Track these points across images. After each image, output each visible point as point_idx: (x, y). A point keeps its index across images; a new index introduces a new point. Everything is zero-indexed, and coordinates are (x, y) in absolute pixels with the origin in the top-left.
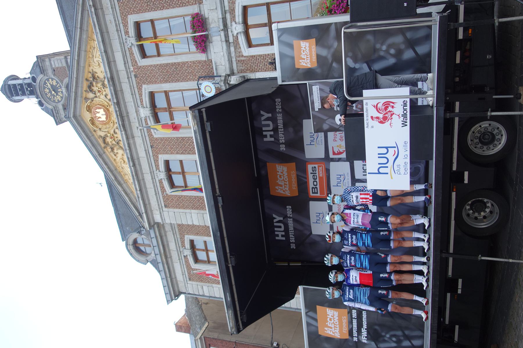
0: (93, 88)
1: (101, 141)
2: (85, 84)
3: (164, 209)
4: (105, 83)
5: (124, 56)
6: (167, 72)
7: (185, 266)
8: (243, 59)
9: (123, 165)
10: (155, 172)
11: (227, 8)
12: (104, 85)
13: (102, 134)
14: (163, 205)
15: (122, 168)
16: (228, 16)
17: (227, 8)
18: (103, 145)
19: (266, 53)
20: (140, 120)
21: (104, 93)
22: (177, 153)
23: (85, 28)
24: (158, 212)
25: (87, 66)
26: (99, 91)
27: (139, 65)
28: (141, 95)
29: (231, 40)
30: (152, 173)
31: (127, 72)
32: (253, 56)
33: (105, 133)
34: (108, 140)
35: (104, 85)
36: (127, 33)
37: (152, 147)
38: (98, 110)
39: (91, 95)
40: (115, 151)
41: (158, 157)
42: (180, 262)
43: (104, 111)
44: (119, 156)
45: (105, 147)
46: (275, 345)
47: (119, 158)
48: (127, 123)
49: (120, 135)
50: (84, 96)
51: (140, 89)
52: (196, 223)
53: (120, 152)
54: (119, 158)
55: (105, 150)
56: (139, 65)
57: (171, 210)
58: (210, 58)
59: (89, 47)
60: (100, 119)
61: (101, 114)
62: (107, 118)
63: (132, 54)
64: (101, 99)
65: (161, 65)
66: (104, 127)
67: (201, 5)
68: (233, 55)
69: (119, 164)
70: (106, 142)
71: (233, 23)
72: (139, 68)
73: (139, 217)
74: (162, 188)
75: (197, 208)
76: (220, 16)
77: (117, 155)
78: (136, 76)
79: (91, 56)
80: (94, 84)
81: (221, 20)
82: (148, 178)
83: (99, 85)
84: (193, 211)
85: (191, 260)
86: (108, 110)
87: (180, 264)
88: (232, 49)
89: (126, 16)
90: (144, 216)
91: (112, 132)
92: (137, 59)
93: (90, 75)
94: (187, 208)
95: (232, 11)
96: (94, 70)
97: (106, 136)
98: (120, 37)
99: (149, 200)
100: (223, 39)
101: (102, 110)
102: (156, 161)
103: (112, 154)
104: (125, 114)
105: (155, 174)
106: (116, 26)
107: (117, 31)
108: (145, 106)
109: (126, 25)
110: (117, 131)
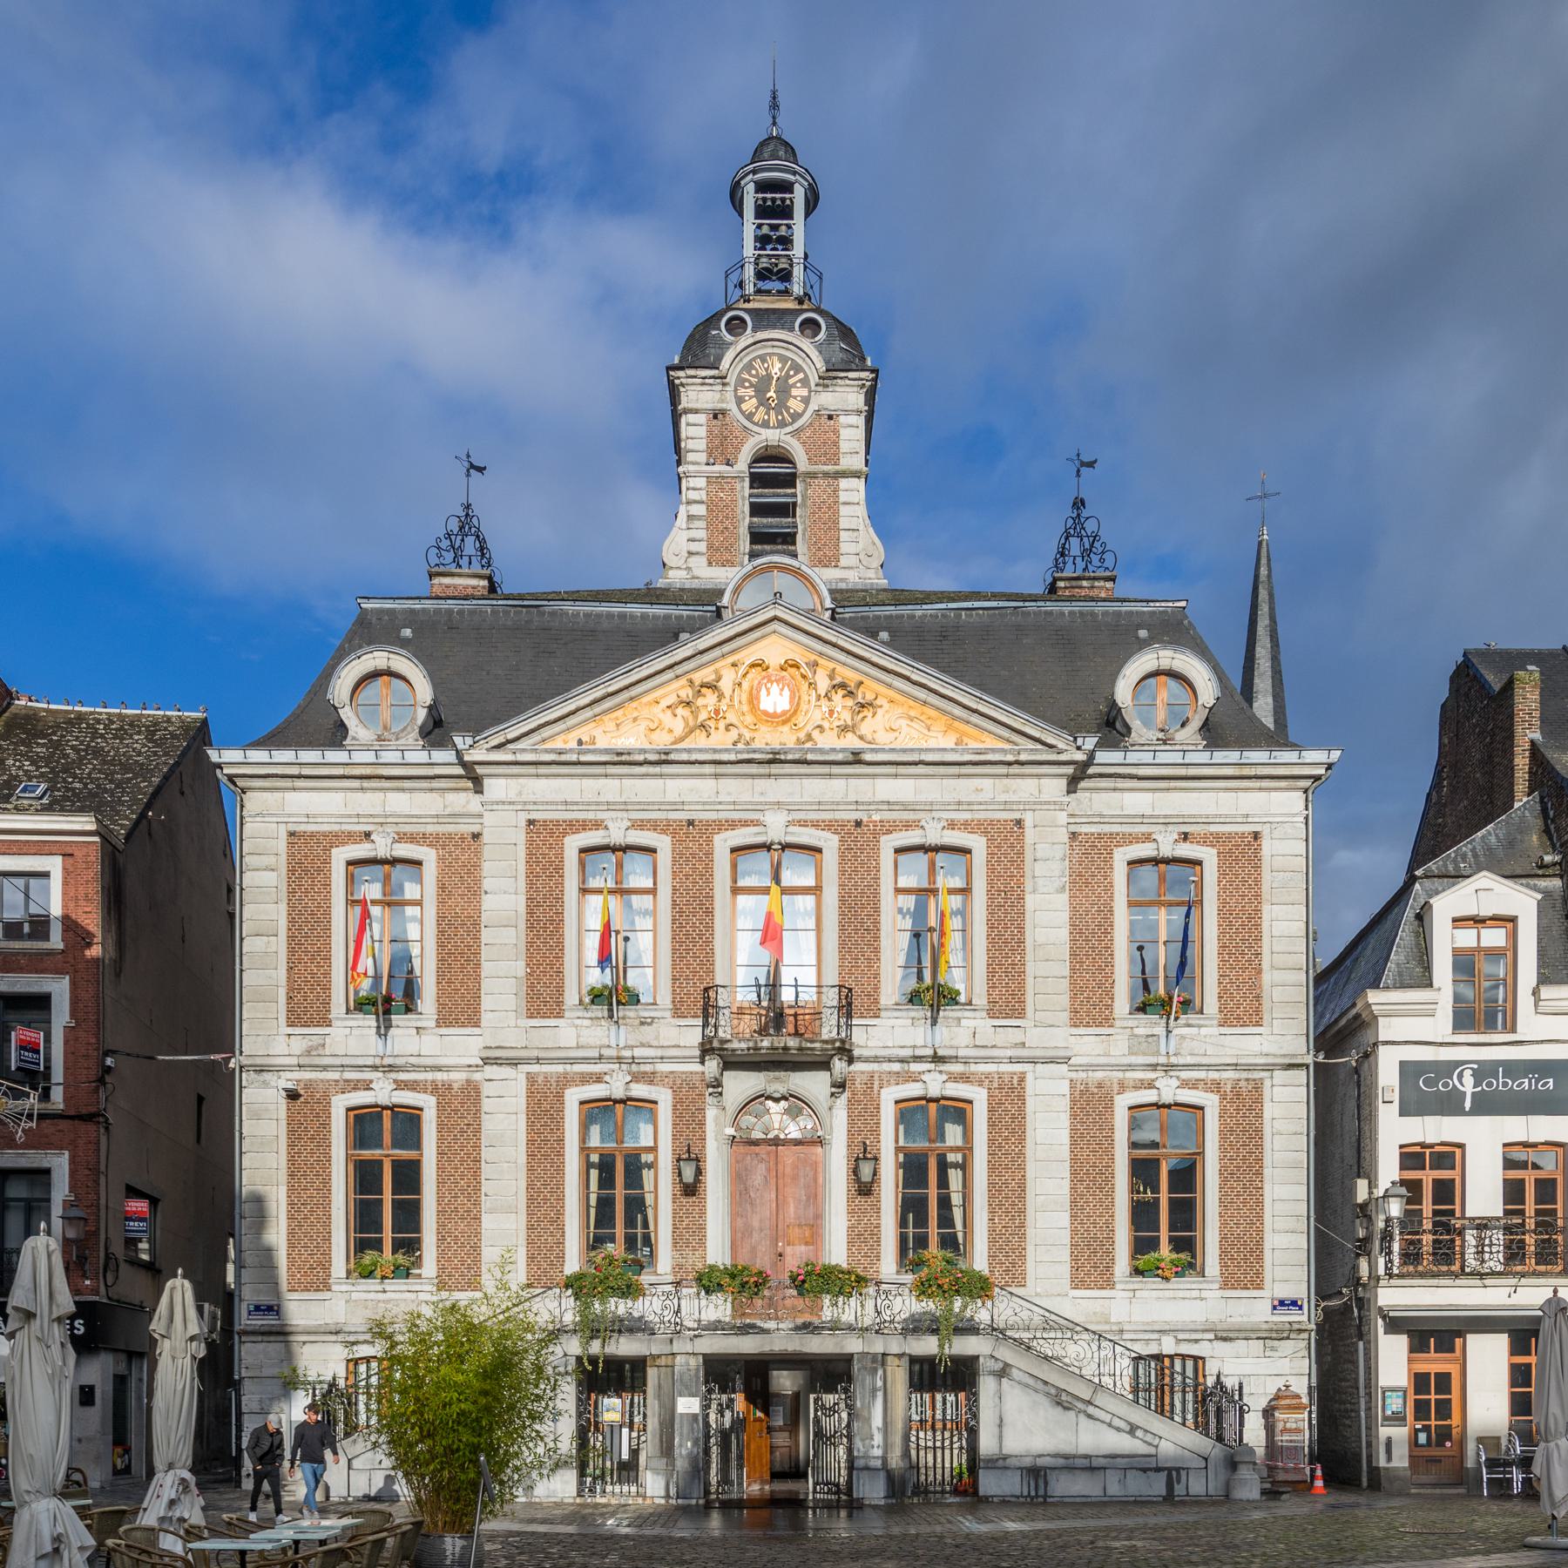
0: (841, 692)
1: (706, 675)
2: (851, 676)
3: (523, 818)
4: (849, 735)
5: (905, 807)
6: (863, 907)
7: (336, 828)
8: (876, 1087)
9: (643, 725)
10: (625, 814)
11: (973, 1068)
12: (844, 729)
13: (726, 685)
14: (533, 816)
15: (635, 719)
16: (957, 1068)
17: (973, 1068)
18: (698, 677)
19: (882, 1138)
20: (760, 808)
21: (826, 725)
22: (674, 889)
23: (975, 719)
24: (512, 796)
25: (892, 693)
26: (831, 712)
27: (883, 839)
28: (816, 825)
29: (915, 1067)
30: (625, 806)
31: (870, 804)
32: (878, 1108)
33: (727, 693)
34: (710, 699)
35: (844, 729)
36: (952, 825)
37: (691, 823)
38: (786, 692)
39: (823, 684)
40: (680, 711)
41: (664, 832)
42: (350, 816)
43: (784, 713)
44: (667, 717)
45: (691, 681)
46: (109, 1061)
47: (661, 716)
48: (754, 769)
49: (720, 739)
50: (821, 661)
51: (829, 826)
52: (488, 903)
53: (679, 727)
54: (661, 716)
55: (683, 681)
56: (883, 839)
57: (521, 837)
58: (883, 1014)
59: (933, 713)
60: (763, 692)
61: (775, 700)
62: (766, 713)
63: (908, 826)
64: (814, 714)
65: (876, 894)
66: (744, 697)
67: (984, 1014)
68: (886, 1067)
69: (645, 713)
70: (704, 690)
71: (945, 1077)
72: (876, 835)
73: (501, 739)
74: (584, 826)
75: (530, 913)
76: (961, 1053)
77: (669, 712)
78: (858, 824)
79: (912, 713)
80: (850, 702)
81: (951, 1052)
82: (609, 788)
83: (846, 717)
84: (522, 900)
85: (361, 851)
86: (784, 722)
87: (342, 816)
88: (896, 1067)
89: (985, 833)
90: (509, 757)
91: (731, 717)
92: (894, 835)
93: (870, 697)
94: (530, 885)
95: (964, 1078)
96: (880, 712)
97: (721, 696)
98: (945, 806)
99: (547, 776)
100: (919, 1052)
101: (787, 707)
102: (654, 826)
103: (672, 699)
104: (775, 769)
105: (620, 814)
106: (969, 804)
107: (959, 803)
108: (791, 829)
109: (966, 826)
110: (734, 734)
